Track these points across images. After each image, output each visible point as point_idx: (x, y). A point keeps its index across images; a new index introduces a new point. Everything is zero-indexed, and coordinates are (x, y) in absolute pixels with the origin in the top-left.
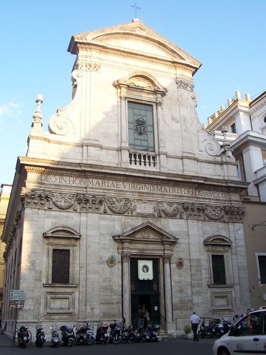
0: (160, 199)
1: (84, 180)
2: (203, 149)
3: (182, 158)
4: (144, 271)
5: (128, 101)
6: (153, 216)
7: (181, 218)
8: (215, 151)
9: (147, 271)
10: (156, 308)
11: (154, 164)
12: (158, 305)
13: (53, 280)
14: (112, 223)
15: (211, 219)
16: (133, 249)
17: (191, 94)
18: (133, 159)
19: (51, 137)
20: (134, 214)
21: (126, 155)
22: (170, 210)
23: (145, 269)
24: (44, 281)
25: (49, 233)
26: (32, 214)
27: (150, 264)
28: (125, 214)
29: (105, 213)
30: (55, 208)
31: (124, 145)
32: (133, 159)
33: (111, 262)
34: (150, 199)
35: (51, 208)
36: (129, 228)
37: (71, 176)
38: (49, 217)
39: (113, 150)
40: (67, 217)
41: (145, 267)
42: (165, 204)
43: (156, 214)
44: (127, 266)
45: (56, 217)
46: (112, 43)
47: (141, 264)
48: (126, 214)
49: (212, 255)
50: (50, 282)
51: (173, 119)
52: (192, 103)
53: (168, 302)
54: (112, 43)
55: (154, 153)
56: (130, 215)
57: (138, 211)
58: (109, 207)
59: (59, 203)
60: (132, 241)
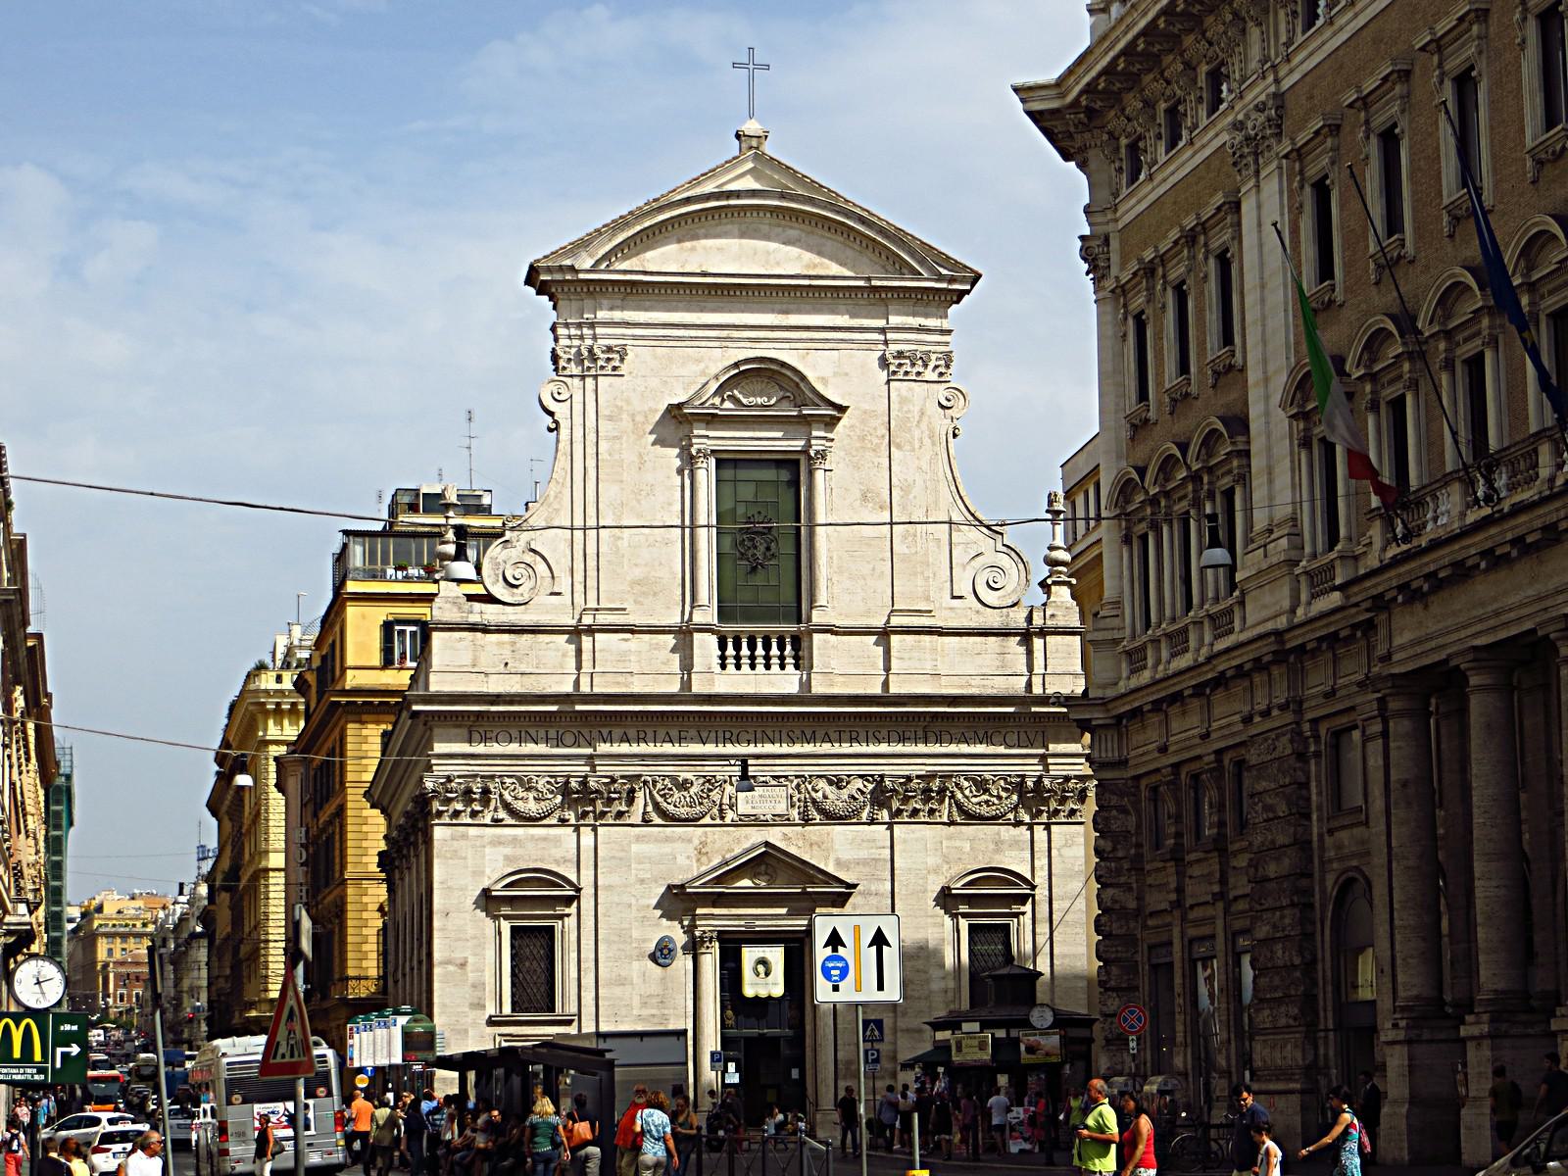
0: (807, 771)
1: (585, 731)
2: (963, 587)
3: (884, 635)
4: (758, 974)
5: (718, 462)
6: (781, 821)
7: (872, 822)
8: (1009, 588)
9: (767, 974)
10: (795, 1073)
11: (797, 658)
12: (800, 1064)
13: (516, 1006)
14: (667, 848)
15: (972, 818)
16: (714, 920)
17: (940, 392)
18: (730, 651)
19: (490, 613)
20: (730, 816)
21: (706, 647)
22: (836, 799)
23: (761, 968)
24: (491, 1010)
25: (499, 886)
26: (453, 839)
27: (776, 955)
28: (701, 822)
29: (646, 822)
30: (509, 821)
31: (699, 618)
32: (730, 651)
33: (662, 954)
34: (779, 771)
35: (502, 820)
36: (716, 862)
37: (551, 727)
38: (498, 842)
39: (669, 632)
40: (545, 839)
41: (763, 962)
42: (822, 784)
43: (795, 814)
44: (711, 961)
45: (515, 840)
46: (665, 260)
47: (749, 955)
48: (707, 820)
49: (972, 928)
50: (507, 1009)
51: (864, 498)
52: (942, 423)
53: (826, 1057)
54: (665, 260)
55: (793, 628)
56: (718, 821)
57: (743, 808)
58: (656, 805)
59: (519, 805)
60: (718, 900)
